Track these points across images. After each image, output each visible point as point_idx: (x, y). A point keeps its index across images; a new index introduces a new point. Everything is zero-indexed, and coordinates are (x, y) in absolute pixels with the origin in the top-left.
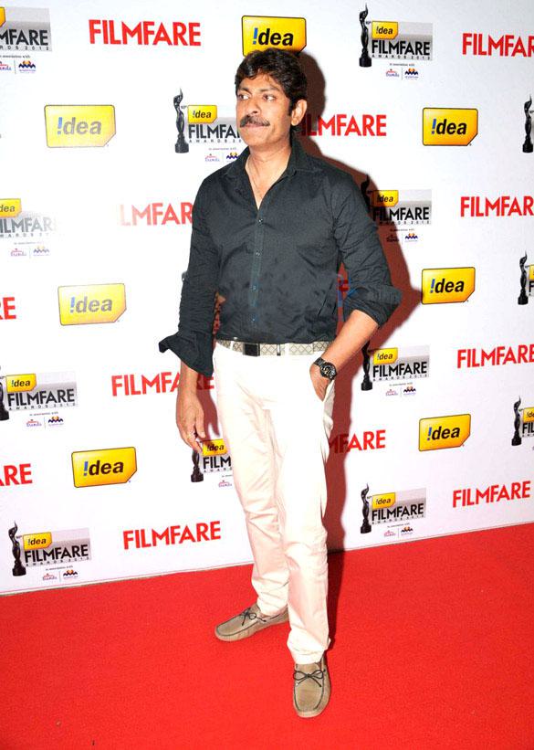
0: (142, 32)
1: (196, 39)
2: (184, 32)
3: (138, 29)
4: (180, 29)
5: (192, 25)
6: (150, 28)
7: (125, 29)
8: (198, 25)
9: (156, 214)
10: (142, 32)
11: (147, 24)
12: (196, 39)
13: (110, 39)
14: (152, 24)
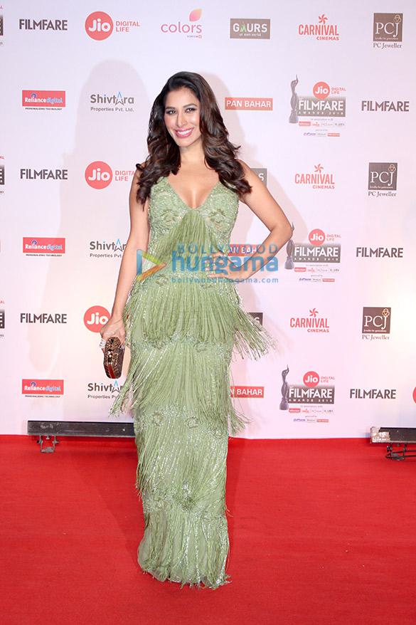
0: (42, 24)
1: (65, 27)
2: (60, 24)
3: (40, 23)
4: (58, 23)
5: (63, 21)
6: (45, 23)
7: (34, 22)
8: (66, 21)
9: (44, 24)
10: (42, 24)
11: (44, 21)
12: (65, 27)
13: (28, 27)
14: (46, 21)
